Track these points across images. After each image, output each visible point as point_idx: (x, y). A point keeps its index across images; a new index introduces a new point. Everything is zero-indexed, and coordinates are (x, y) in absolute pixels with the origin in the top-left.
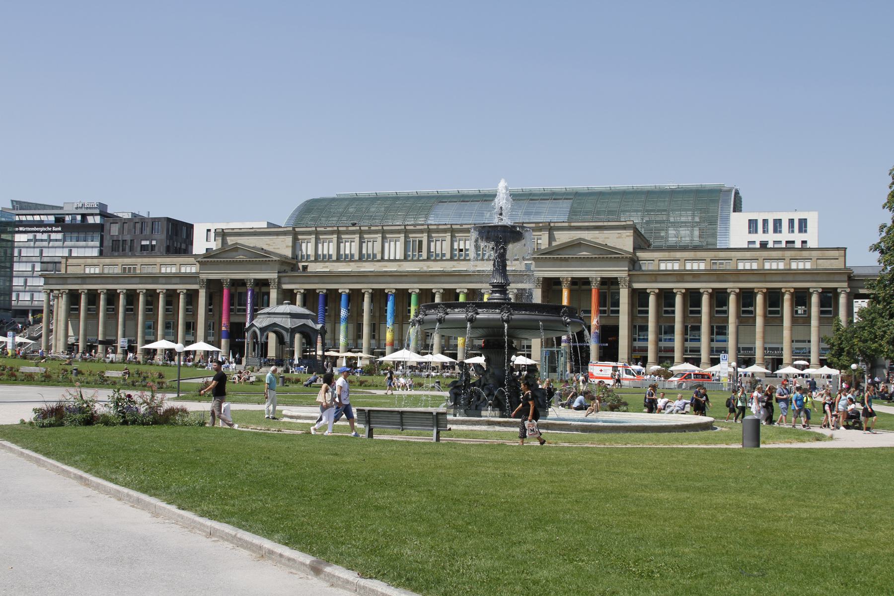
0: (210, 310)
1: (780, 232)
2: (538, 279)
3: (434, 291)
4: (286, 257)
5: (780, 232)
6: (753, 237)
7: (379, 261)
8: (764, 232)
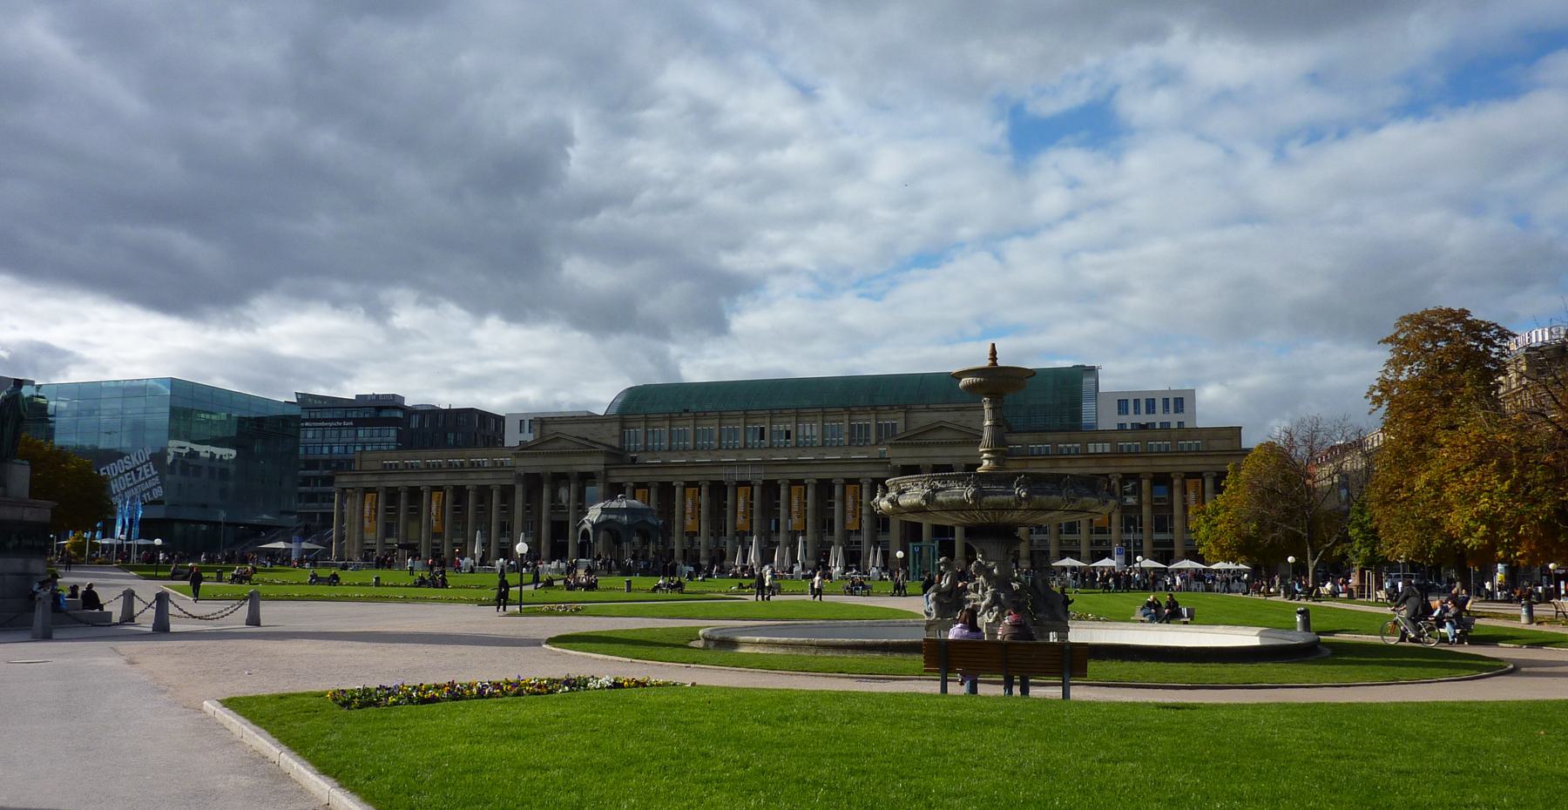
0: (528, 508)
1: (1154, 412)
2: (896, 467)
3: (779, 482)
4: (614, 448)
5: (1154, 412)
6: (1124, 419)
7: (716, 450)
8: (1135, 413)
